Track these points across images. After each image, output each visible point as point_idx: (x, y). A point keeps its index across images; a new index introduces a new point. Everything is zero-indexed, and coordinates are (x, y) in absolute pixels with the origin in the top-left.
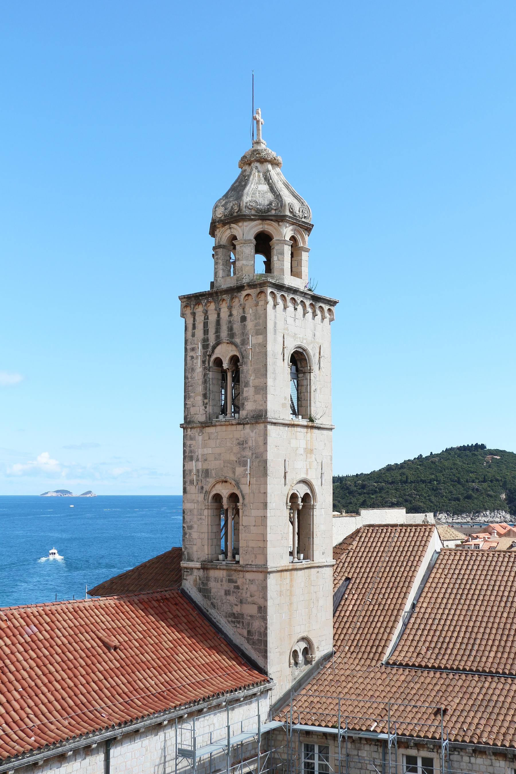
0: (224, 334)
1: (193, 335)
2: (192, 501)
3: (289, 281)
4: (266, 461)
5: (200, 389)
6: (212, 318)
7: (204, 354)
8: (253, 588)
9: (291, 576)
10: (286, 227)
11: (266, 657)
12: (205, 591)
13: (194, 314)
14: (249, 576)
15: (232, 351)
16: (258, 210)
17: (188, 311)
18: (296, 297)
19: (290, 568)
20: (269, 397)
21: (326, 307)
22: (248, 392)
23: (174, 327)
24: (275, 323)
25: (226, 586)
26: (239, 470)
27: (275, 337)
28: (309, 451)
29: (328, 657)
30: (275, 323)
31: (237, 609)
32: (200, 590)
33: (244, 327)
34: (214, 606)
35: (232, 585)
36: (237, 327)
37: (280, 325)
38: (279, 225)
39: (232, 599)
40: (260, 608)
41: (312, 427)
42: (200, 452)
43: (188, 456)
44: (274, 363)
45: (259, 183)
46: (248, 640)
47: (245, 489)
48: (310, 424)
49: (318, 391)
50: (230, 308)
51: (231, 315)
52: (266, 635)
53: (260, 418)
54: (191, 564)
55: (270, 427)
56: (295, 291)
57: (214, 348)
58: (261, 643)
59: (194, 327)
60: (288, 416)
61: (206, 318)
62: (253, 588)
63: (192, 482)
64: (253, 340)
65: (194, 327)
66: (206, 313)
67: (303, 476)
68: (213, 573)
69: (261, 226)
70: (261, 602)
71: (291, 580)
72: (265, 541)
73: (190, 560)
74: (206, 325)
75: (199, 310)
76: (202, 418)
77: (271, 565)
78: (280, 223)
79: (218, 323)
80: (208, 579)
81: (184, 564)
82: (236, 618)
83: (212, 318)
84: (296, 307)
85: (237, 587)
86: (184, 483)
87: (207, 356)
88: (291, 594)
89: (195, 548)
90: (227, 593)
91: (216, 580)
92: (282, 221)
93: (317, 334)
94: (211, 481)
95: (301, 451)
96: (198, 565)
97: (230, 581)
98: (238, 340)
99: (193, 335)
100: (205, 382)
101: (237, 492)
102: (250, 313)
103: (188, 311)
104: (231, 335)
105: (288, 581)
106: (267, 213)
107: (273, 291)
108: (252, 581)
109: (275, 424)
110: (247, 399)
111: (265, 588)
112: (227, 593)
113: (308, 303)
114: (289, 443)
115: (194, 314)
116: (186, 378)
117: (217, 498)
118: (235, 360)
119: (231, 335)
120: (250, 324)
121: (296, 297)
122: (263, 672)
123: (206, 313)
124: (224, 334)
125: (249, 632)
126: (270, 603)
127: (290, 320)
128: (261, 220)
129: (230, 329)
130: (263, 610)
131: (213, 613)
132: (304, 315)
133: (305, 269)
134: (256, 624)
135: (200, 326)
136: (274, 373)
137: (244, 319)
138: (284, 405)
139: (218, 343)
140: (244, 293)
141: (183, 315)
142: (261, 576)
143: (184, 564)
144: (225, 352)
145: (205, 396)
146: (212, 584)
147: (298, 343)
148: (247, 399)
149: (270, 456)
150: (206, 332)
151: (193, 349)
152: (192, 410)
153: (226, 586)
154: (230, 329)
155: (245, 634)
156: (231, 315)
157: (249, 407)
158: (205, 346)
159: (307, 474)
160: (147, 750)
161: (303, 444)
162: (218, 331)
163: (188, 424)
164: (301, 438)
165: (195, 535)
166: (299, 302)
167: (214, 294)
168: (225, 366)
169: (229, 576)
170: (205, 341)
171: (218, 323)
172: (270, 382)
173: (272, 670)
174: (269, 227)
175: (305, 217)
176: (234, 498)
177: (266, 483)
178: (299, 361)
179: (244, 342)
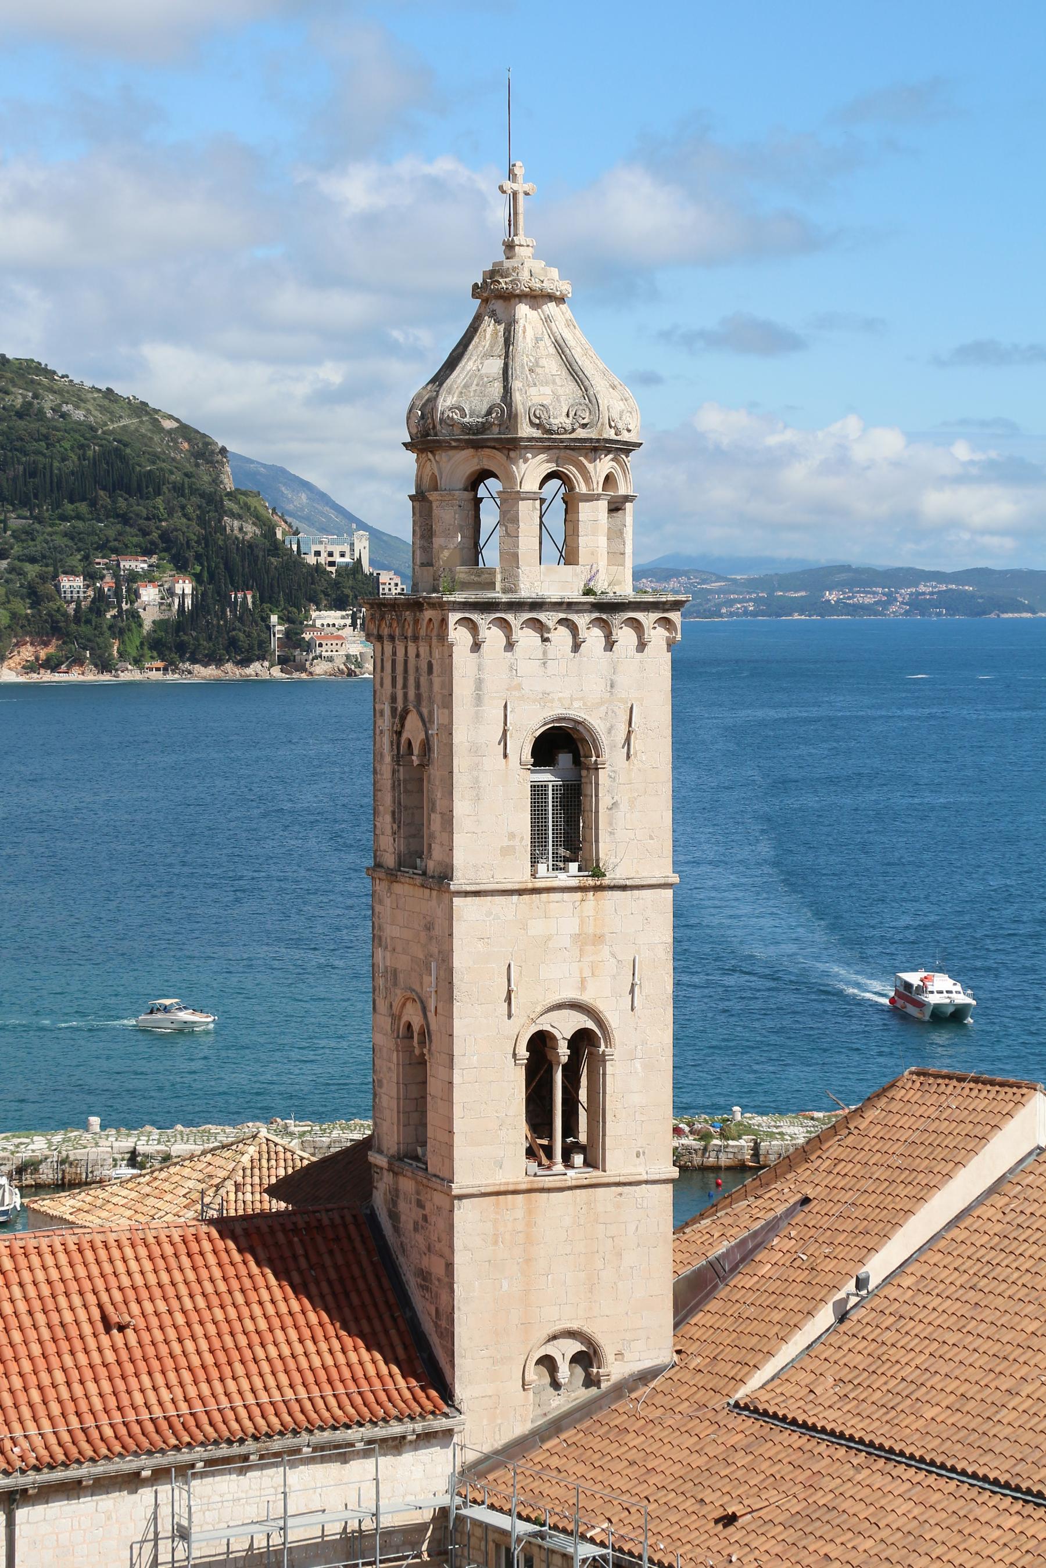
5: (387, 798)
10: (526, 461)
12: (394, 1216)
16: (467, 429)
18: (542, 616)
19: (524, 1187)
24: (479, 683)
27: (477, 713)
28: (589, 940)
29: (645, 1377)
30: (479, 683)
35: (421, 1212)
38: (508, 457)
41: (597, 888)
45: (488, 355)
46: (436, 1325)
48: (591, 882)
49: (623, 807)
55: (457, 901)
56: (537, 605)
69: (476, 460)
71: (530, 1212)
72: (451, 1132)
73: (380, 1151)
78: (512, 454)
84: (546, 635)
85: (425, 1218)
92: (515, 449)
93: (619, 679)
105: (519, 1213)
106: (482, 433)
107: (467, 615)
109: (467, 894)
113: (582, 620)
114: (525, 927)
121: (542, 616)
122: (447, 1394)
125: (437, 1310)
128: (473, 448)
129: (418, 686)
132: (576, 647)
136: (476, 785)
138: (507, 851)
147: (558, 711)
154: (418, 686)
158: (394, 710)
159: (583, 987)
160: (109, 1518)
162: (405, 686)
166: (551, 624)
169: (418, 1193)
173: (461, 1391)
175: (584, 426)
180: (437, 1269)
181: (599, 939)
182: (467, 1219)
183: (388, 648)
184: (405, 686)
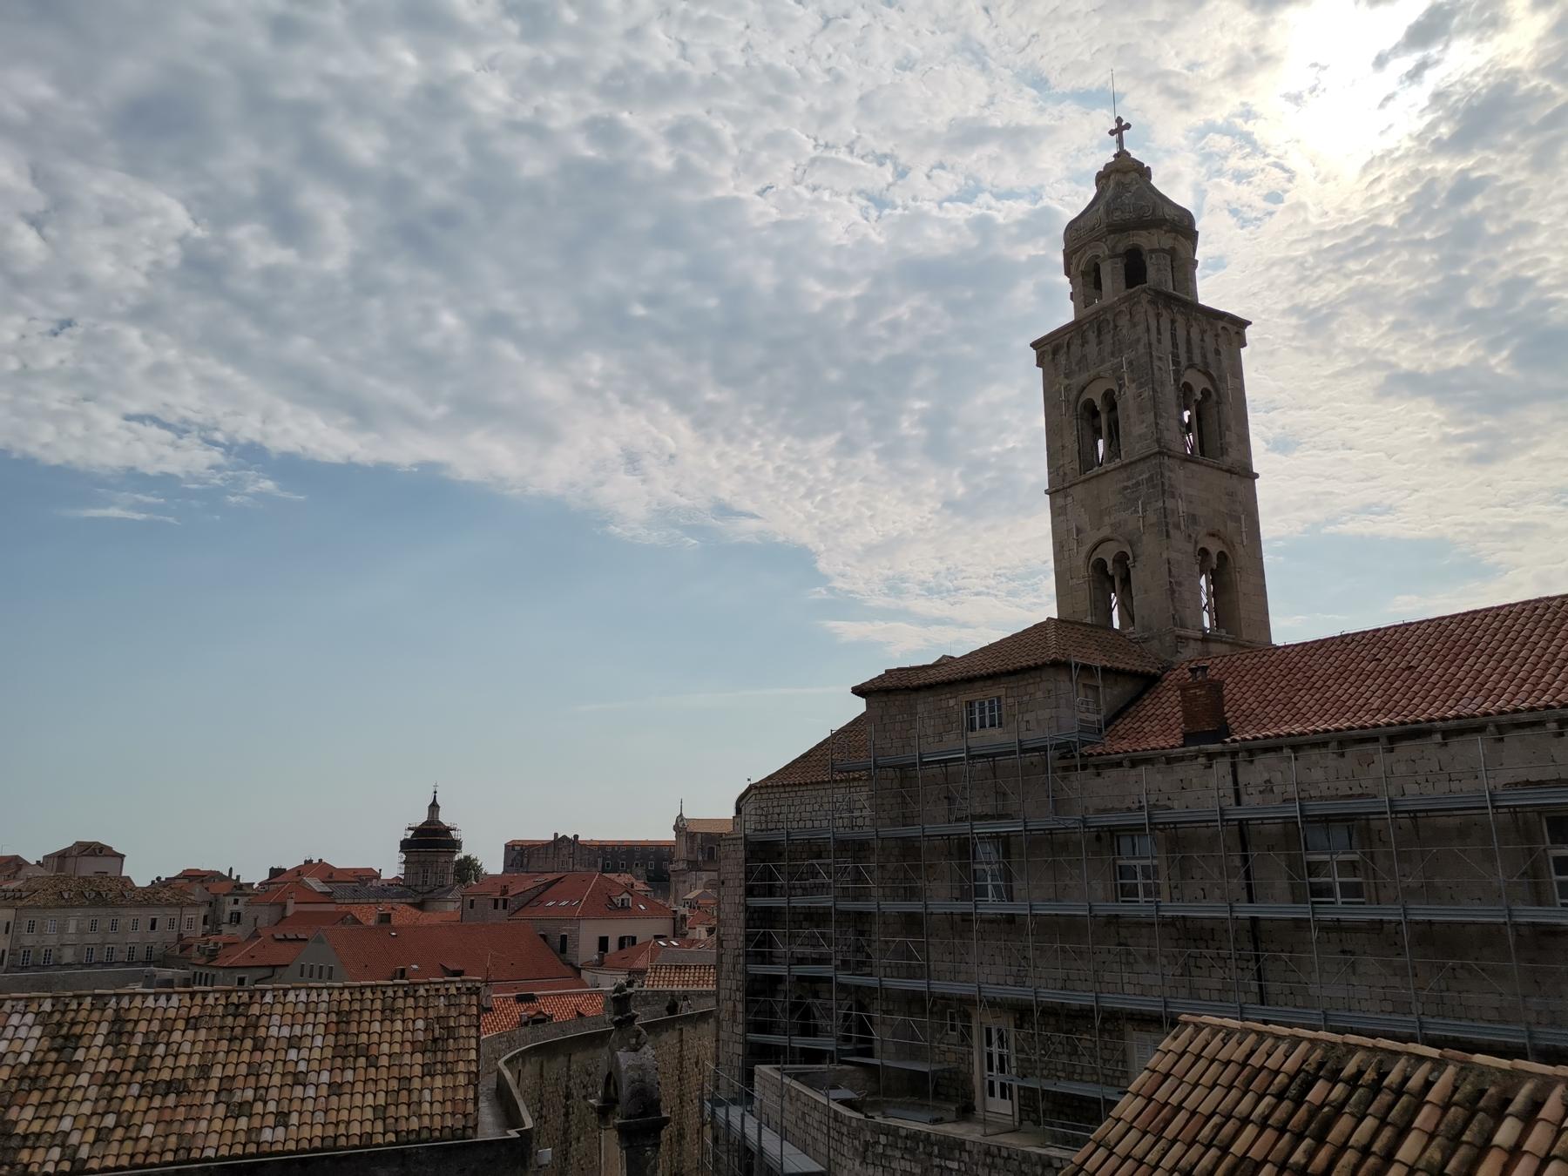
1: (1159, 341)
13: (1158, 316)
36: (1211, 357)
74: (1173, 336)
79: (1189, 341)
83: (1181, 333)
99: (1159, 341)
102: (1223, 349)
115: (1158, 316)
120: (1225, 363)
124: (1197, 359)
129: (1204, 356)
137: (1218, 352)
140: (1221, 324)
154: (1204, 356)
171: (1189, 341)
184: (1189, 351)
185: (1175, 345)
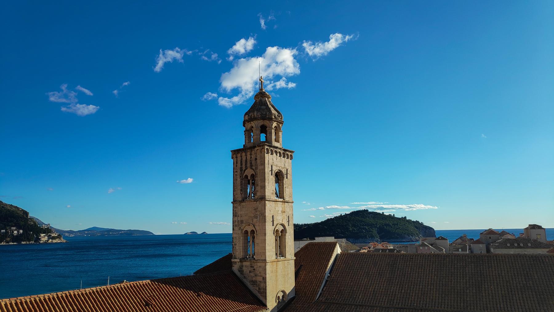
0: (248, 165)
2: (236, 234)
3: (275, 144)
4: (265, 216)
5: (239, 187)
6: (244, 159)
7: (241, 174)
8: (261, 269)
9: (276, 264)
11: (266, 299)
12: (241, 270)
13: (237, 157)
14: (259, 264)
15: (252, 172)
17: (235, 156)
20: (266, 190)
21: (290, 154)
22: (258, 188)
23: (230, 163)
25: (250, 269)
26: (255, 220)
31: (254, 279)
32: (239, 271)
33: (256, 162)
34: (245, 277)
36: (253, 162)
37: (271, 162)
39: (252, 274)
40: (263, 278)
42: (239, 213)
43: (235, 215)
44: (268, 177)
46: (259, 292)
47: (257, 228)
50: (251, 154)
51: (251, 158)
52: (266, 290)
53: (263, 198)
54: (236, 260)
56: (277, 148)
57: (245, 171)
58: (264, 292)
59: (237, 163)
60: (274, 198)
61: (242, 159)
62: (261, 269)
63: (236, 226)
64: (260, 167)
65: (237, 163)
66: (241, 156)
67: (281, 222)
68: (244, 264)
70: (264, 275)
72: (265, 249)
73: (235, 258)
74: (241, 162)
75: (239, 155)
76: (240, 199)
77: (268, 259)
79: (246, 161)
80: (242, 266)
81: (233, 260)
82: (254, 283)
83: (244, 159)
85: (254, 269)
86: (233, 226)
87: (241, 174)
88: (277, 272)
89: (237, 253)
90: (250, 272)
91: (246, 266)
94: (244, 225)
95: (280, 212)
96: (239, 260)
97: (252, 267)
98: (254, 168)
100: (241, 185)
101: (254, 229)
103: (235, 156)
104: (251, 166)
105: (275, 266)
108: (260, 267)
110: (257, 191)
111: (265, 270)
112: (250, 272)
115: (237, 157)
116: (234, 183)
117: (246, 232)
118: (253, 176)
119: (251, 166)
120: (258, 161)
123: (241, 156)
124: (248, 165)
125: (259, 288)
126: (267, 276)
127: (275, 159)
129: (251, 163)
130: (264, 279)
131: (244, 280)
133: (281, 139)
134: (262, 285)
135: (239, 162)
137: (256, 159)
138: (272, 193)
139: (246, 169)
140: (256, 149)
141: (232, 158)
142: (264, 264)
143: (233, 260)
144: (249, 172)
145: (241, 190)
146: (244, 268)
148: (257, 191)
149: (267, 214)
150: (241, 165)
151: (236, 172)
152: (236, 196)
153: (250, 269)
154: (251, 163)
155: (257, 288)
156: (251, 158)
157: (259, 194)
158: (241, 170)
161: (281, 209)
163: (234, 202)
164: (280, 206)
165: (237, 248)
167: (245, 149)
168: (249, 178)
170: (241, 168)
171: (246, 161)
172: (266, 184)
174: (266, 123)
176: (253, 232)
177: (265, 225)
178: (279, 177)
179: (256, 168)
180: (259, 279)
181: (284, 212)
182: (269, 267)
183: (239, 159)
185: (241, 165)
